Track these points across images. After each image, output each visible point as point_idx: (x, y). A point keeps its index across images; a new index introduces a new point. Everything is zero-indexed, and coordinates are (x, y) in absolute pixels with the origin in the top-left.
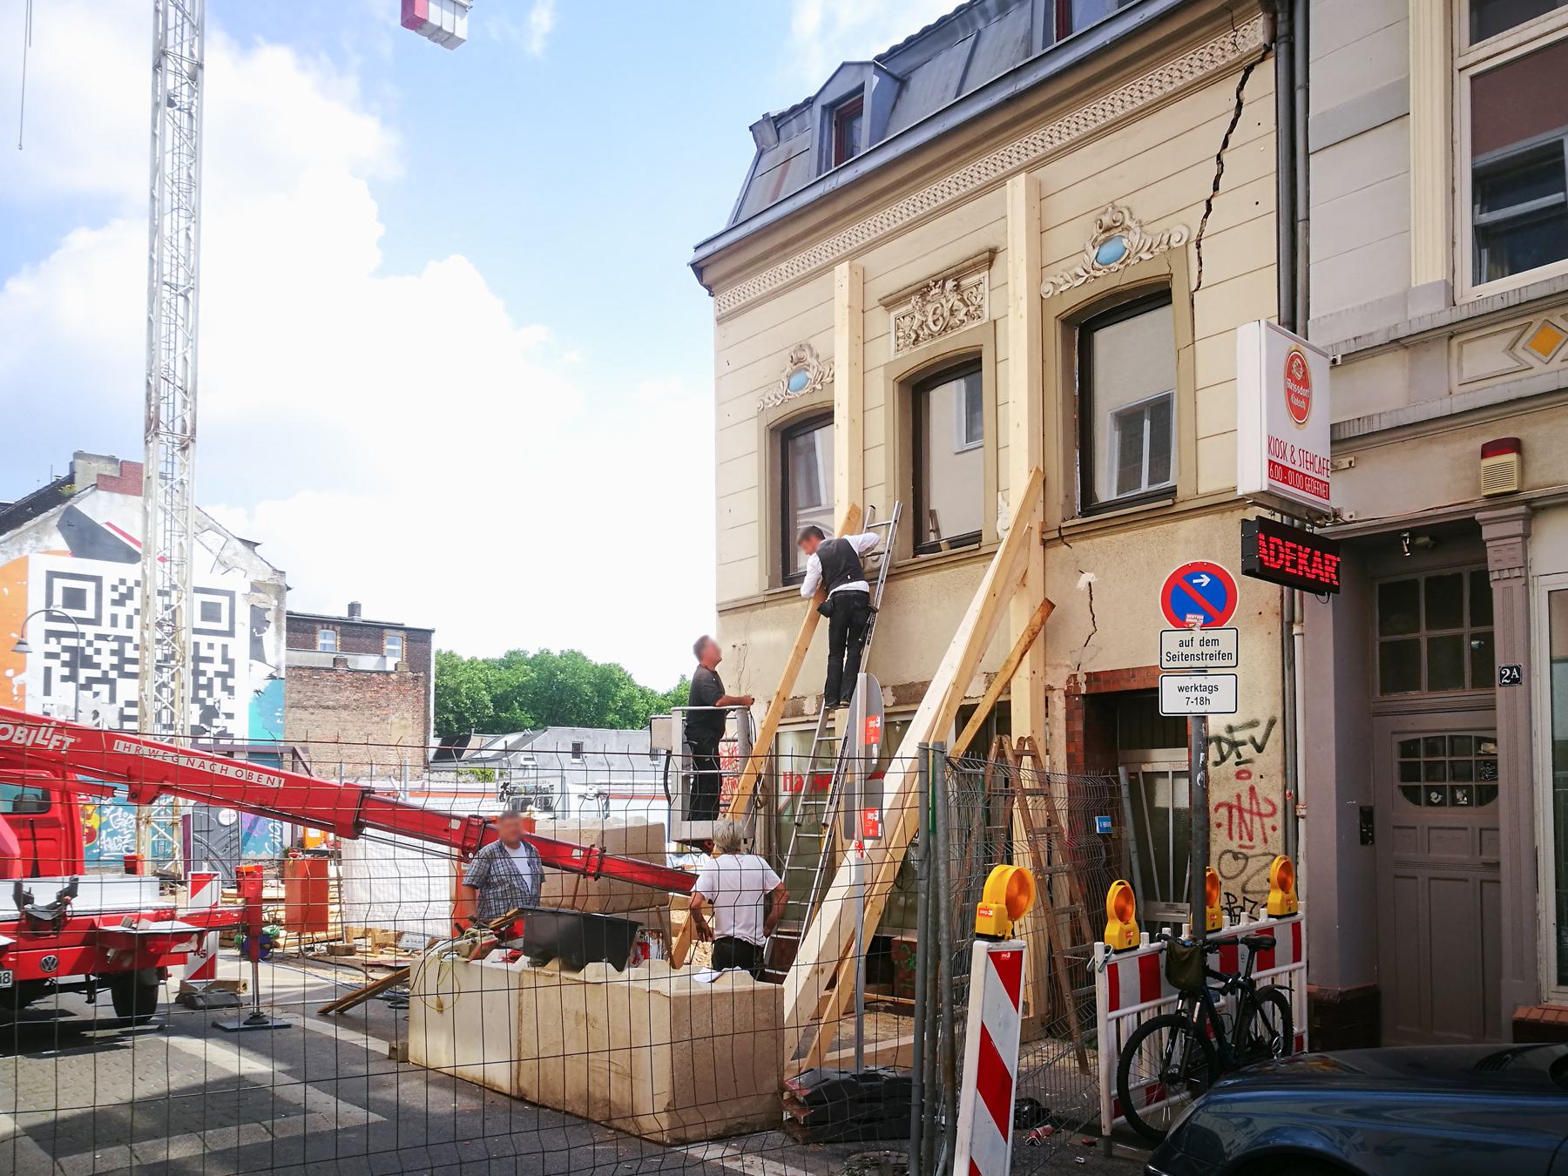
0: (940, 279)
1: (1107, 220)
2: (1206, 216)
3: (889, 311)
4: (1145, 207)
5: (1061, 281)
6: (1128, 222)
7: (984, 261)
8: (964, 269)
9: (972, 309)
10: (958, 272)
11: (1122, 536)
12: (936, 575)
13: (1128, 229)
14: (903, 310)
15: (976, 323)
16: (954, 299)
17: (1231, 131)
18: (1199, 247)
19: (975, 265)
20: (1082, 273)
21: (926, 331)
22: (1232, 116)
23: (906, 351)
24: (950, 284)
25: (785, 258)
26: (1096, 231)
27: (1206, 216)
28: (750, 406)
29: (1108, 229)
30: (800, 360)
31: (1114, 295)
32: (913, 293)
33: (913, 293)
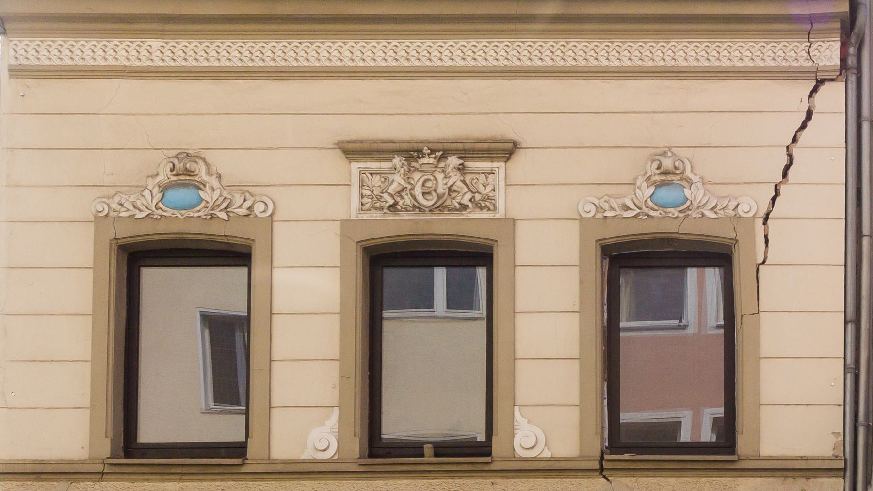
0: (442, 151)
1: (667, 163)
2: (774, 199)
5: (606, 206)
6: (688, 173)
7: (504, 150)
8: (474, 151)
9: (478, 197)
10: (465, 150)
11: (673, 480)
12: (419, 482)
13: (690, 183)
14: (374, 165)
15: (485, 215)
16: (455, 178)
17: (803, 126)
18: (765, 223)
19: (489, 151)
20: (632, 206)
21: (408, 200)
22: (803, 116)
23: (376, 215)
24: (453, 161)
25: (161, 34)
26: (652, 169)
27: (774, 199)
28: (89, 204)
29: (666, 173)
30: (188, 172)
31: (666, 240)
32: (399, 152)
33: (399, 152)
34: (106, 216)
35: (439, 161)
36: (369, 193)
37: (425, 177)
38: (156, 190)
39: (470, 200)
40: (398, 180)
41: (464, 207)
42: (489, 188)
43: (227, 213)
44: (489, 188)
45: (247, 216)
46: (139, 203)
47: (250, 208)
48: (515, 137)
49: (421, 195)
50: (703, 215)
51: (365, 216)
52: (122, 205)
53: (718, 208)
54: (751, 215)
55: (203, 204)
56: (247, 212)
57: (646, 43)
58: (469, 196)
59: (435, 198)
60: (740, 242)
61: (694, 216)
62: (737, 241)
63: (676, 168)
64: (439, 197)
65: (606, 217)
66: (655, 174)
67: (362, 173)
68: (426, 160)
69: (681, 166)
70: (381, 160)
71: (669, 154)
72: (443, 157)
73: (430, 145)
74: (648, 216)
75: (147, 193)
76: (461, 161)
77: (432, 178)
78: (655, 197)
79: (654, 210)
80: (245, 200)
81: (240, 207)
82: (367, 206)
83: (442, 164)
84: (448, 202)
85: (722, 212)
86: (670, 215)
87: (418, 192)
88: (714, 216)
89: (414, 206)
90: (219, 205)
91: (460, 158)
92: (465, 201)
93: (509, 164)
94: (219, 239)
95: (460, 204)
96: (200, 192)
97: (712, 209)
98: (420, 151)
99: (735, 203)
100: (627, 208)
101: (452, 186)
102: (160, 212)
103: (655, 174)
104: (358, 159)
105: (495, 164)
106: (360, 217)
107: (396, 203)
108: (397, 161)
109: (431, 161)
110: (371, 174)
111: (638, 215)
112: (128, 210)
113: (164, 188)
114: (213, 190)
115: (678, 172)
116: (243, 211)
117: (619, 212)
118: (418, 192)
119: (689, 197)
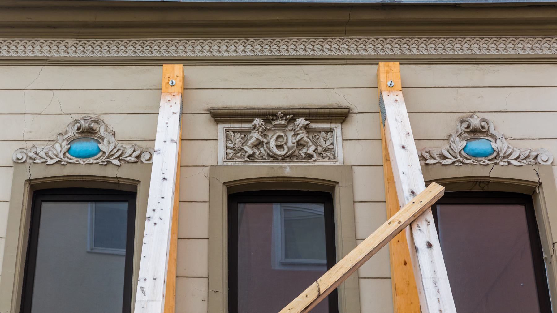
0: (291, 115)
1: (475, 122)
3: (217, 122)
4: (500, 125)
5: (427, 155)
14: (237, 126)
20: (448, 156)
23: (238, 163)
24: (301, 121)
34: (24, 162)
35: (288, 123)
36: (232, 146)
37: (278, 134)
38: (65, 143)
39: (314, 151)
40: (255, 135)
41: (311, 156)
42: (328, 143)
43: (120, 160)
44: (328, 143)
45: (136, 162)
46: (50, 154)
47: (138, 157)
48: (349, 105)
49: (275, 147)
50: (509, 163)
51: (229, 164)
52: (37, 154)
53: (522, 157)
54: (549, 163)
55: (101, 154)
56: (136, 160)
57: (447, 39)
58: (313, 148)
59: (286, 150)
60: (543, 184)
61: (501, 163)
62: (540, 184)
63: (483, 127)
64: (289, 150)
65: (427, 164)
66: (465, 132)
67: (227, 131)
68: (279, 122)
69: (486, 126)
70: (242, 122)
71: (475, 117)
72: (292, 120)
73: (283, 111)
74: (463, 163)
75: (57, 146)
76: (306, 122)
77: (283, 135)
78: (467, 149)
79: (467, 159)
80: (134, 151)
81: (130, 156)
82: (230, 156)
83: (290, 127)
84: (296, 153)
85: (524, 161)
86: (481, 163)
87: (273, 144)
88: (519, 164)
89: (269, 155)
90: (113, 155)
91: (306, 120)
92: (311, 150)
93: (344, 125)
94: (112, 181)
95: (306, 153)
96: (100, 145)
97: (516, 159)
98: (275, 115)
99: (536, 154)
100: (444, 157)
101: (299, 140)
102: (66, 159)
103: (465, 132)
104: (223, 122)
105: (333, 125)
106: (225, 164)
107: (254, 153)
108: (257, 121)
109: (283, 122)
110: (234, 132)
111: (454, 162)
112: (41, 158)
113: (71, 141)
114: (110, 143)
115: (484, 130)
116: (132, 159)
117: (438, 160)
118: (273, 144)
119: (496, 149)
